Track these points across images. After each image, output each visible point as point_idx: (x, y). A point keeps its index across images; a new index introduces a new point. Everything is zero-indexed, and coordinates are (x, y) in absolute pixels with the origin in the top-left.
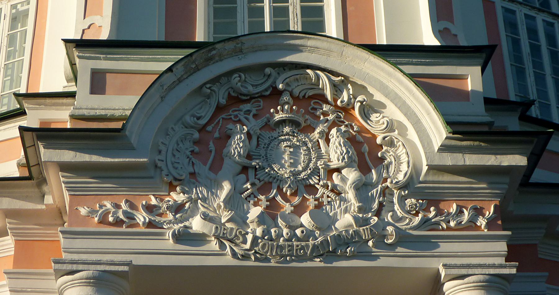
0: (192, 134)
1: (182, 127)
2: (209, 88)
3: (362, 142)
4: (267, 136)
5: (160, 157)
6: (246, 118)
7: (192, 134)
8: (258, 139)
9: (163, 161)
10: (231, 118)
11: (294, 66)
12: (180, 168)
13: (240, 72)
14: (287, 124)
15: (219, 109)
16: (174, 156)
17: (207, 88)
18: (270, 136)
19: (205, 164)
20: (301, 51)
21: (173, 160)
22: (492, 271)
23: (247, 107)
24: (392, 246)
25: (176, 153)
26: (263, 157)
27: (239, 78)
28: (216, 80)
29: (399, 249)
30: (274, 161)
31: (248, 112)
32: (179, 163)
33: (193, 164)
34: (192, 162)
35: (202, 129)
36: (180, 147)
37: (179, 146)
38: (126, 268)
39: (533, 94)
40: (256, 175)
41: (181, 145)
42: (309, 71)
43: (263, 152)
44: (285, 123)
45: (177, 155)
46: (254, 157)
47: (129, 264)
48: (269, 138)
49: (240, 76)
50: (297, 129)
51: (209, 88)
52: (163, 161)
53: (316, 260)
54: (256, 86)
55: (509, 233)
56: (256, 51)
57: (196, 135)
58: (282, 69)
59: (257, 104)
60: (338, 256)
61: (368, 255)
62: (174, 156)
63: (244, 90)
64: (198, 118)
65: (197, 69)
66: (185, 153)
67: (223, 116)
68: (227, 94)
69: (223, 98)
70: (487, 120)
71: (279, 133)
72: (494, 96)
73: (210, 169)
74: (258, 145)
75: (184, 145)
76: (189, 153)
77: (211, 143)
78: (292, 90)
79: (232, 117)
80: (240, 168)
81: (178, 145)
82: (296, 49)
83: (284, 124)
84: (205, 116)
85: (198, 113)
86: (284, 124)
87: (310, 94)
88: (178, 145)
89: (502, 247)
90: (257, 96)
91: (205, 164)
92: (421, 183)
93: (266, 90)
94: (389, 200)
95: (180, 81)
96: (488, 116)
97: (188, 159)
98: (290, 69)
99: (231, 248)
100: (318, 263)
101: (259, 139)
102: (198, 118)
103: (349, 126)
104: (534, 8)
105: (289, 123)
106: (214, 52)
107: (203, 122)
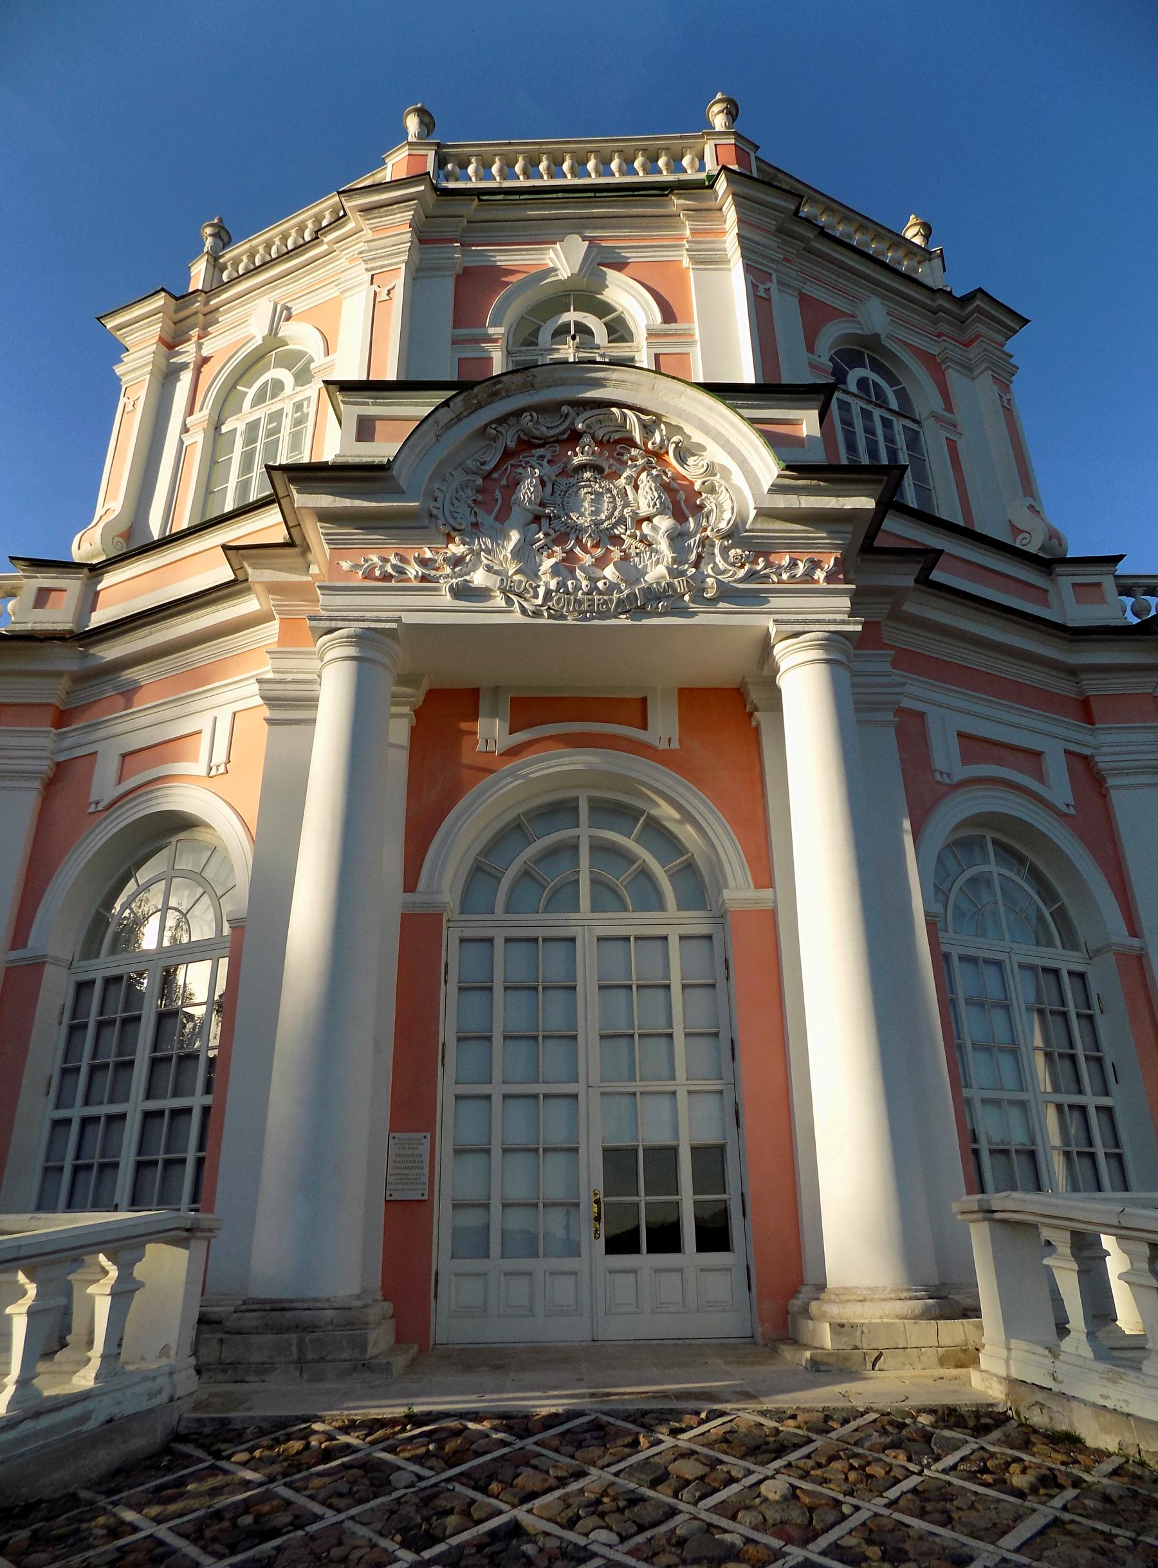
0: (475, 481)
7: (475, 481)
8: (553, 485)
14: (588, 468)
15: (507, 454)
16: (453, 505)
20: (605, 386)
21: (452, 509)
22: (833, 628)
23: (541, 451)
24: (713, 601)
25: (454, 501)
28: (502, 420)
29: (721, 605)
31: (542, 457)
35: (487, 477)
38: (394, 625)
40: (550, 525)
41: (461, 493)
42: (614, 410)
45: (457, 504)
47: (398, 620)
49: (531, 415)
51: (495, 429)
53: (622, 616)
54: (552, 428)
56: (551, 386)
57: (480, 481)
58: (581, 408)
60: (648, 612)
61: (684, 612)
62: (453, 505)
63: (537, 433)
65: (480, 406)
68: (516, 437)
73: (496, 519)
74: (553, 492)
76: (470, 501)
77: (497, 492)
80: (531, 517)
81: (457, 492)
82: (598, 384)
87: (616, 437)
88: (457, 492)
89: (845, 602)
90: (552, 439)
92: (747, 531)
93: (563, 433)
99: (520, 604)
100: (623, 620)
102: (483, 464)
104: (871, 402)
106: (499, 386)
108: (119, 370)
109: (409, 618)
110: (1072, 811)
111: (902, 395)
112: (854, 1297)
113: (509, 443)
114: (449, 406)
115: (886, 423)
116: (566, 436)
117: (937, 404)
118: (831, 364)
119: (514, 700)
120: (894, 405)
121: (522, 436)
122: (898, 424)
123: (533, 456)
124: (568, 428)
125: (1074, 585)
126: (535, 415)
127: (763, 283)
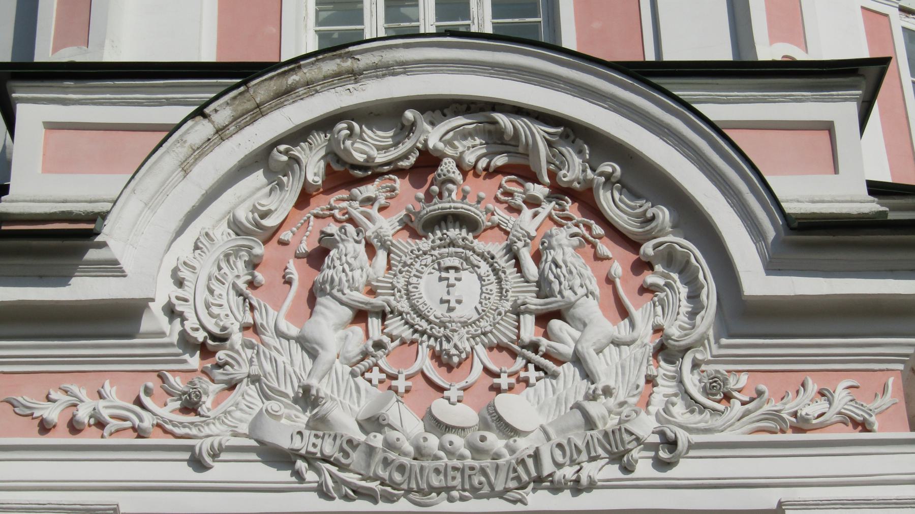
0: (251, 248)
1: (229, 234)
2: (286, 152)
3: (608, 258)
4: (407, 249)
5: (180, 293)
7: (251, 248)
8: (388, 255)
9: (186, 300)
10: (333, 216)
11: (464, 107)
12: (222, 316)
13: (353, 120)
16: (211, 292)
17: (280, 152)
18: (415, 248)
19: (278, 308)
25: (215, 285)
26: (399, 291)
27: (348, 132)
30: (421, 298)
31: (370, 201)
32: (221, 305)
33: (252, 308)
34: (250, 304)
36: (225, 273)
37: (222, 271)
41: (225, 269)
43: (401, 282)
44: (446, 222)
46: (379, 291)
48: (412, 252)
49: (350, 128)
50: (470, 234)
51: (286, 152)
52: (186, 300)
58: (438, 113)
59: (387, 187)
62: (211, 292)
63: (360, 158)
64: (265, 215)
66: (234, 286)
67: (317, 210)
69: (315, 174)
70: (873, 210)
71: (433, 242)
72: (886, 177)
74: (390, 267)
75: (233, 269)
76: (243, 287)
78: (462, 153)
79: (336, 213)
80: (348, 313)
81: (220, 269)
83: (443, 224)
84: (276, 210)
85: (263, 206)
86: (443, 224)
88: (220, 269)
91: (278, 308)
93: (405, 156)
94: (666, 372)
95: (221, 133)
96: (873, 201)
97: (241, 298)
98: (456, 114)
101: (392, 255)
102: (265, 215)
103: (581, 226)
105: (455, 222)
107: (270, 222)
113: (310, 178)
114: (205, 116)
116: (413, 159)
123: (352, 199)
126: (356, 126)
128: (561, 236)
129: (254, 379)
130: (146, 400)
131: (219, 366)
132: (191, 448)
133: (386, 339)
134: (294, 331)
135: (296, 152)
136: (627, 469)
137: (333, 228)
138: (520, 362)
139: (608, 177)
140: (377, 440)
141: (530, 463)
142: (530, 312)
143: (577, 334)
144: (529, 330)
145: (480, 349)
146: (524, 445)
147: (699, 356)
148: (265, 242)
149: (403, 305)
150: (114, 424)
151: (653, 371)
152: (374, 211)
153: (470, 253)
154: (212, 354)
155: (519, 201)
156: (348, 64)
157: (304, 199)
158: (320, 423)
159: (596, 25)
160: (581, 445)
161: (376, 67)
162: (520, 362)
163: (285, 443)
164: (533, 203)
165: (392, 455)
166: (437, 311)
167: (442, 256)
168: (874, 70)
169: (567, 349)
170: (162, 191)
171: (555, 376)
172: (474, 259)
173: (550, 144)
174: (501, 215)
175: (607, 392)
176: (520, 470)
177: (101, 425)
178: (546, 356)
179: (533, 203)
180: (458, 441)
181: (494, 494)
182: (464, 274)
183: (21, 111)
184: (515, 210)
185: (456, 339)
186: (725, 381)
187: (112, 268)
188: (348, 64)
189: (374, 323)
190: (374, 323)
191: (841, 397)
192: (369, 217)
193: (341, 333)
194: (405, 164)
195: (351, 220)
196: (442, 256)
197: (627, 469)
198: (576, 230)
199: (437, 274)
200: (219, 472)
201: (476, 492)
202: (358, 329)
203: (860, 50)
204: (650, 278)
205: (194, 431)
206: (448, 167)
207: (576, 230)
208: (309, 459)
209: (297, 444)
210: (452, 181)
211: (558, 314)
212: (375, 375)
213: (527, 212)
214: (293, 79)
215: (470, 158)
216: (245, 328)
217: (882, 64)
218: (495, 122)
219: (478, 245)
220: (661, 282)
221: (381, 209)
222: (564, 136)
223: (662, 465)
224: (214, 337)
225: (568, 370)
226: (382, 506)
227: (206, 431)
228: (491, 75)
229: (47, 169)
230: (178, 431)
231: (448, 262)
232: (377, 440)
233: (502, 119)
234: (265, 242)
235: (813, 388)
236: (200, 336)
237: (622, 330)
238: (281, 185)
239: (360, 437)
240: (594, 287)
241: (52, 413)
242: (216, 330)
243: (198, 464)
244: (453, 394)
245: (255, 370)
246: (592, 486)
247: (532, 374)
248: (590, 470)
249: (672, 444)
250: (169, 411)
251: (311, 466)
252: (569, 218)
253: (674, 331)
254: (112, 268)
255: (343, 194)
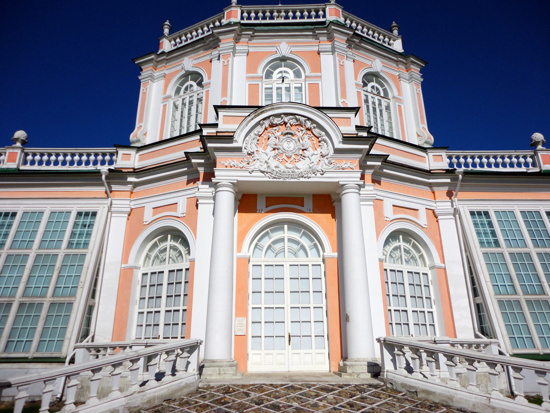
2: (262, 122)
5: (246, 145)
6: (275, 132)
21: (251, 146)
23: (275, 128)
28: (264, 119)
31: (275, 130)
39: (372, 124)
49: (273, 118)
51: (262, 122)
55: (362, 171)
63: (275, 123)
72: (359, 125)
80: (273, 149)
91: (261, 147)
93: (282, 123)
98: (290, 115)
104: (374, 94)
107: (260, 133)
108: (140, 78)
109: (240, 179)
110: (426, 227)
111: (385, 91)
112: (354, 360)
115: (380, 101)
117: (396, 94)
118: (362, 84)
119: (267, 198)
120: (382, 95)
121: (270, 124)
122: (384, 102)
123: (273, 129)
124: (283, 121)
125: (433, 155)
127: (342, 59)
128: (306, 136)
129: (258, 159)
130: (241, 163)
131: (253, 157)
132: (248, 170)
133: (278, 153)
134: (264, 152)
135: (264, 122)
136: (316, 175)
137: (270, 135)
138: (299, 157)
139: (314, 127)
140: (277, 170)
141: (301, 174)
142: (301, 149)
143: (308, 153)
144: (301, 152)
145: (293, 155)
146: (300, 171)
147: (327, 157)
148: (259, 136)
149: (281, 148)
150: (236, 166)
151: (320, 159)
152: (276, 131)
153: (291, 139)
154: (251, 155)
155: (299, 130)
156: (272, 107)
157: (266, 129)
158: (268, 167)
159: (312, 94)
160: (308, 171)
161: (277, 108)
162: (299, 157)
163: (263, 170)
164: (302, 131)
165: (279, 172)
166: (287, 149)
167: (287, 140)
168: (358, 109)
169: (306, 155)
170: (243, 128)
171: (305, 160)
172: (292, 140)
173: (305, 121)
174: (297, 133)
175: (313, 162)
176: (299, 175)
177: (234, 166)
178: (303, 156)
179: (302, 131)
180: (290, 171)
181: (295, 178)
182: (290, 143)
183: (220, 113)
184: (299, 132)
185: (289, 153)
186: (331, 161)
187: (236, 141)
188: (272, 107)
189: (276, 150)
190: (276, 150)
191: (349, 164)
192: (275, 132)
193: (271, 152)
194: (282, 124)
195: (273, 133)
196: (287, 140)
197: (316, 175)
198: (308, 136)
199: (287, 143)
200: (253, 174)
201: (292, 178)
202: (274, 151)
203: (356, 105)
204: (320, 144)
205: (249, 168)
206: (288, 125)
207: (308, 136)
208: (267, 172)
209: (265, 170)
210: (289, 127)
211: (305, 150)
212: (277, 159)
213: (301, 132)
214: (264, 109)
215: (292, 123)
216: (257, 151)
217: (359, 108)
218: (296, 117)
219: (293, 138)
220: (322, 144)
221: (278, 131)
222: (307, 120)
223: (321, 174)
224: (252, 153)
225: (307, 159)
226: (278, 180)
227: (250, 167)
228: (297, 109)
229: (223, 123)
230: (246, 167)
231: (288, 141)
232: (277, 170)
233: (297, 117)
234: (259, 136)
235: (345, 162)
236: (249, 152)
237: (316, 152)
238: (262, 127)
239: (274, 169)
240: (311, 146)
241: (226, 164)
242: (252, 152)
243: (249, 172)
244: (289, 162)
245: (258, 158)
246: (310, 177)
247: (301, 159)
248: (309, 175)
249: (323, 171)
250: (244, 164)
251: (267, 173)
252: (307, 133)
253: (324, 153)
254: (236, 141)
255: (271, 128)
